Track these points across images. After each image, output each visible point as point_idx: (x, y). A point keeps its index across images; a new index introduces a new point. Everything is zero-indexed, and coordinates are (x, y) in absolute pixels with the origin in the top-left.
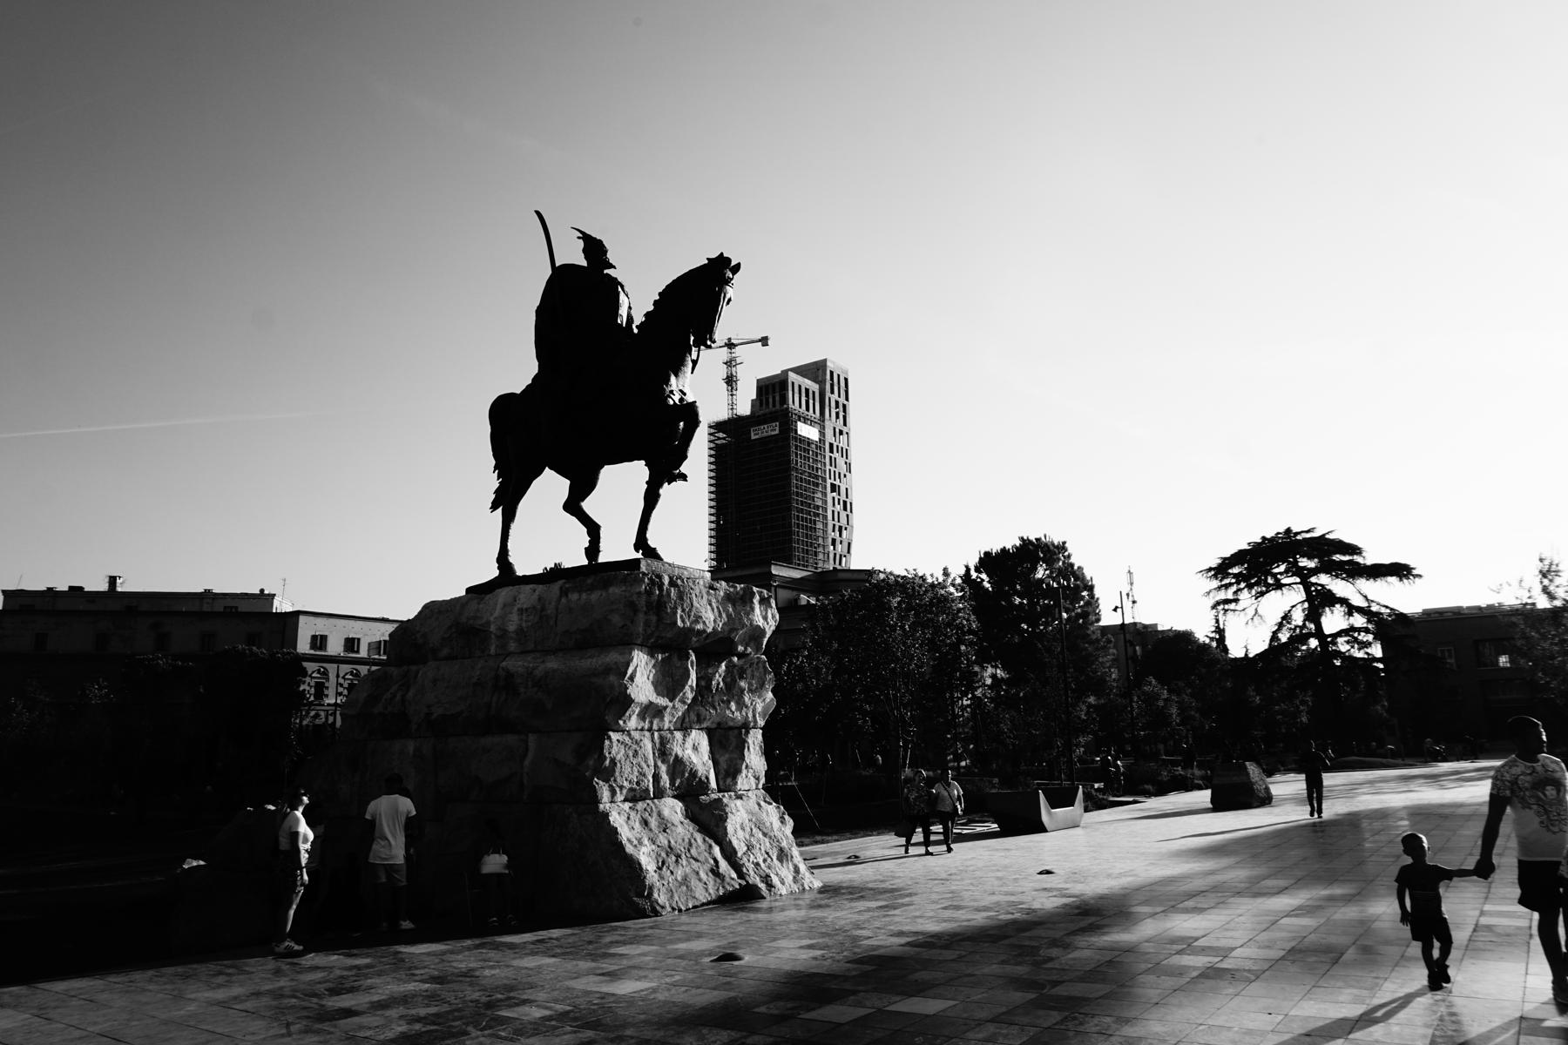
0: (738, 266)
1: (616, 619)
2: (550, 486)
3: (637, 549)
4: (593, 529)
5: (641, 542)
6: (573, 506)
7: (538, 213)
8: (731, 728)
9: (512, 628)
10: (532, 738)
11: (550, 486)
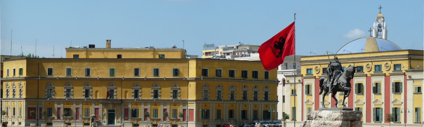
9: (326, 117)
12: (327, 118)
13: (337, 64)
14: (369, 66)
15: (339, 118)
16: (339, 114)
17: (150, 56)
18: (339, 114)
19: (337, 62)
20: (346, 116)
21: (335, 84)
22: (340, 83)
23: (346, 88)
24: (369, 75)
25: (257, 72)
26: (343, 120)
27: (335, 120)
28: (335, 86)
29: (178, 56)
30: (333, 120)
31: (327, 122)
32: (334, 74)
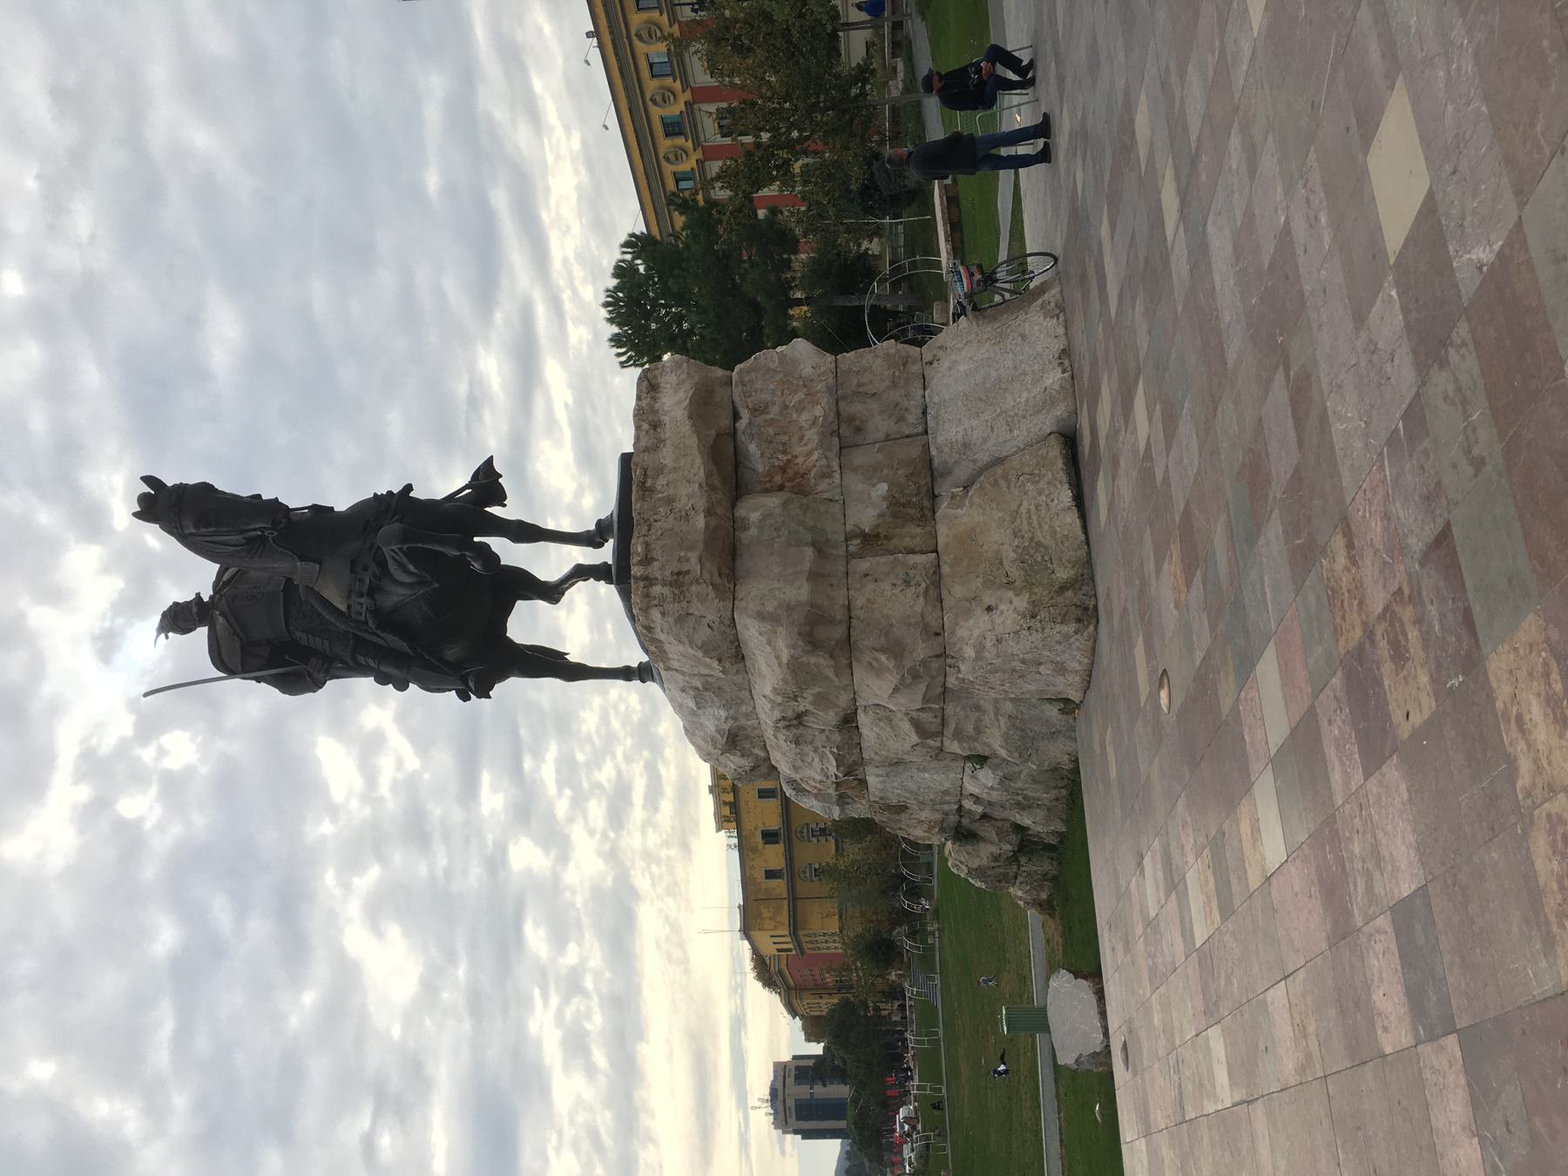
0: (148, 480)
1: (703, 634)
2: (527, 624)
3: (599, 545)
4: (581, 573)
5: (592, 539)
6: (552, 592)
7: (146, 695)
8: (838, 413)
9: (723, 714)
10: (861, 702)
11: (527, 624)
22: (376, 612)
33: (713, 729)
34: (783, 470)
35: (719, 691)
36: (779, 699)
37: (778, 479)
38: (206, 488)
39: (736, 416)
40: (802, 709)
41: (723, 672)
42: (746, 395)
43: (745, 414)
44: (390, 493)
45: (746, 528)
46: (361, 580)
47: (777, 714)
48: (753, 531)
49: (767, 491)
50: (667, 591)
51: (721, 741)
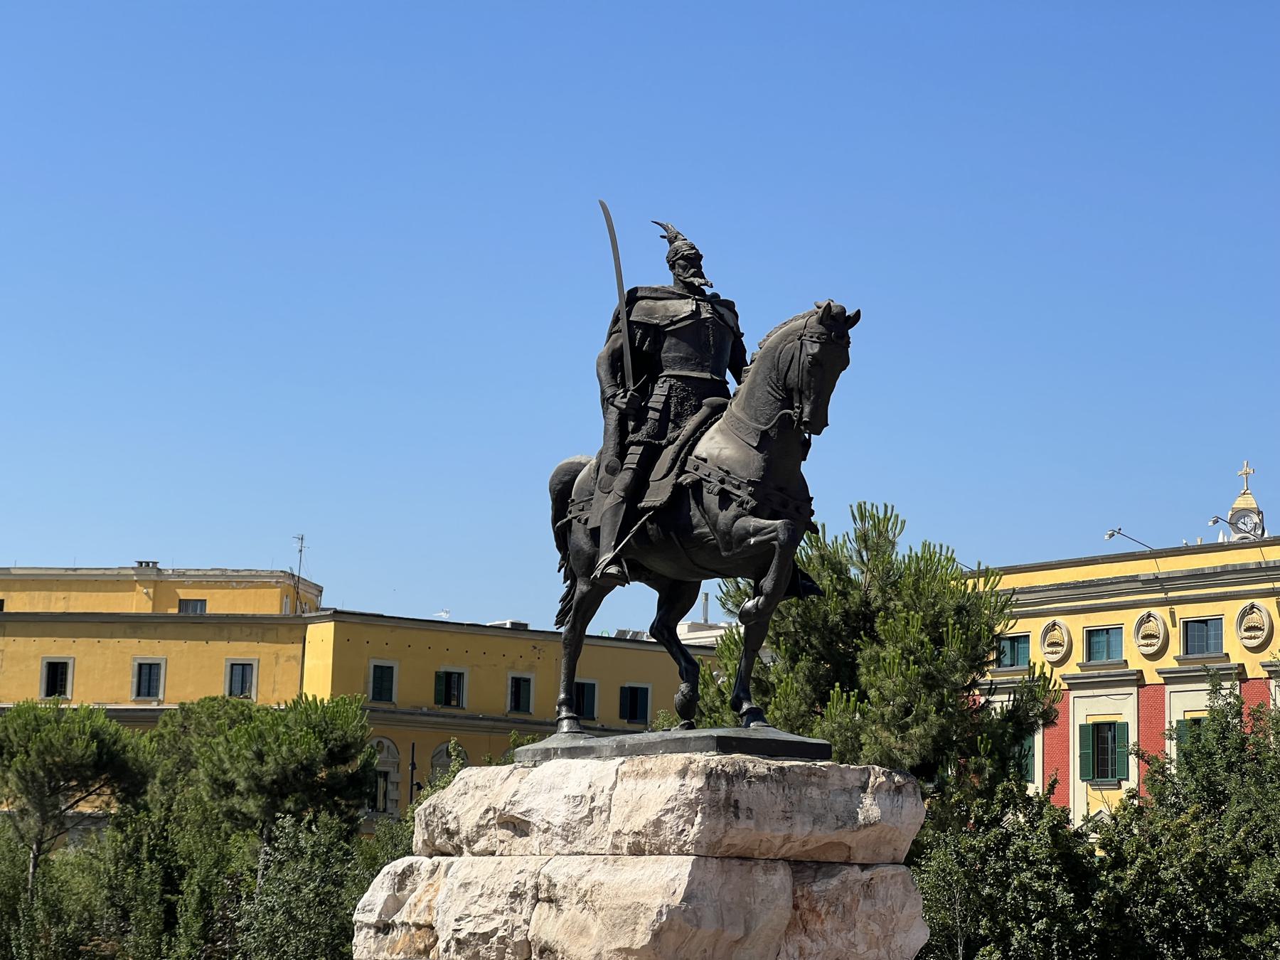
0: (858, 314)
9: (558, 821)
12: (568, 832)
13: (686, 307)
14: (1150, 627)
15: (667, 834)
16: (672, 784)
17: (136, 602)
18: (672, 784)
19: (694, 291)
20: (732, 807)
21: (657, 495)
22: (697, 485)
23: (753, 522)
24: (1151, 678)
25: (645, 691)
26: (711, 854)
27: (637, 851)
28: (658, 511)
29: (268, 603)
30: (615, 850)
31: (563, 870)
32: (657, 400)
33: (533, 805)
34: (813, 910)
35: (588, 819)
36: (584, 885)
37: (805, 905)
38: (845, 362)
39: (864, 867)
40: (565, 906)
41: (618, 833)
42: (883, 879)
43: (867, 875)
44: (812, 513)
45: (766, 871)
46: (739, 488)
47: (560, 879)
48: (761, 878)
49: (794, 892)
50: (722, 795)
51: (516, 811)
